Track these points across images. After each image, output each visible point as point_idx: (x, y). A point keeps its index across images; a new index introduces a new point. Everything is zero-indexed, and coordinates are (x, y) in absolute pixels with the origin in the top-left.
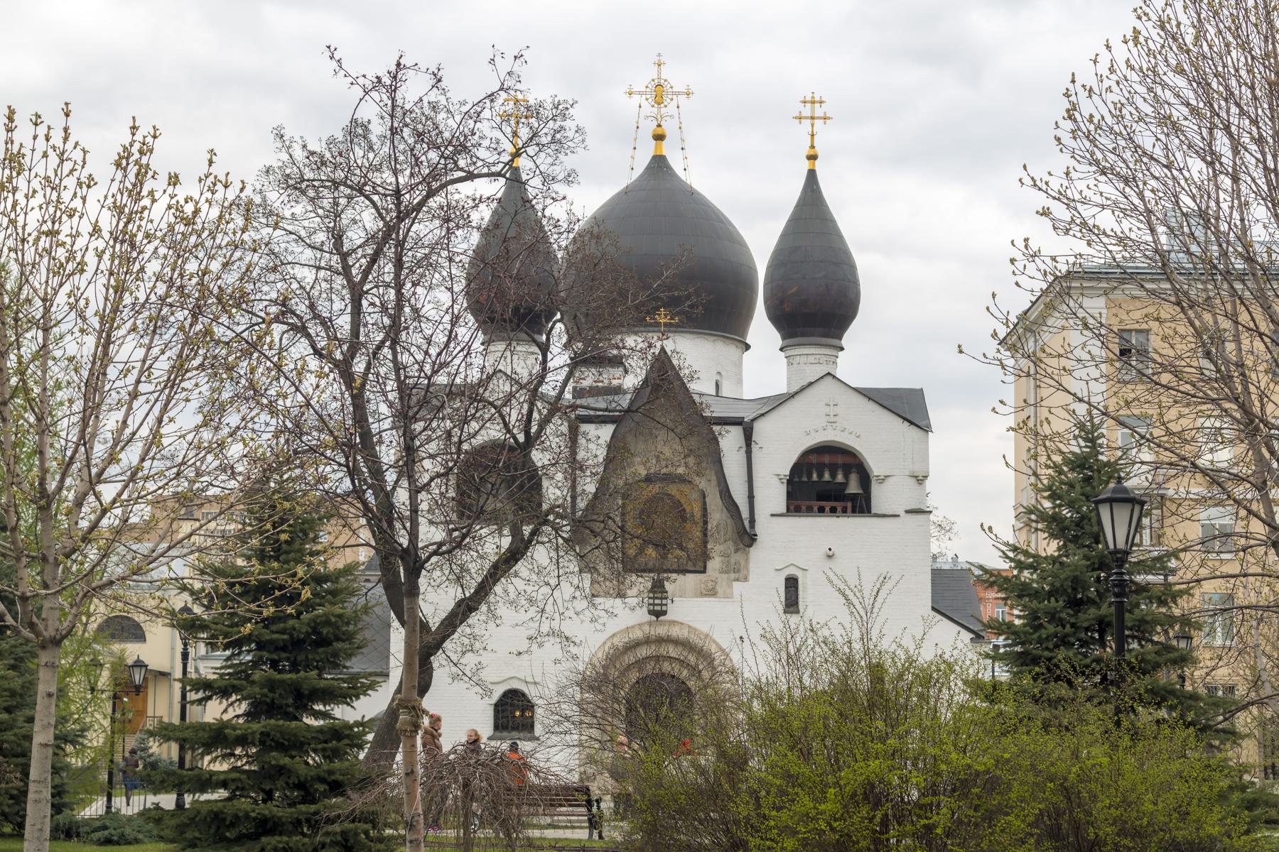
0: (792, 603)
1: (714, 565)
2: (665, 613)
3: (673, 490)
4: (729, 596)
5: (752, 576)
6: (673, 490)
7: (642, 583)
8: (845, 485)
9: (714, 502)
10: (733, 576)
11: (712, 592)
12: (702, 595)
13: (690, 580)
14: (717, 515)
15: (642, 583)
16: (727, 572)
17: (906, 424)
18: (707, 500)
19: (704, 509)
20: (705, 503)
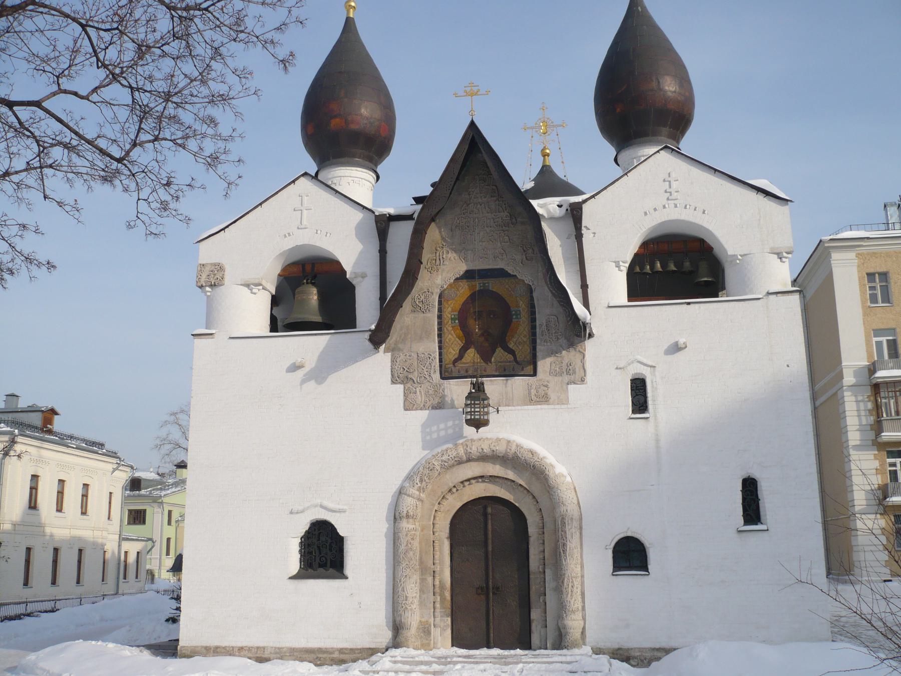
0: (640, 403)
1: (544, 365)
2: (485, 423)
3: (493, 285)
4: (563, 401)
5: (589, 377)
6: (493, 285)
7: (458, 390)
8: (693, 273)
9: (542, 294)
10: (566, 378)
11: (544, 399)
12: (531, 402)
13: (519, 383)
14: (546, 311)
15: (458, 390)
16: (561, 374)
17: (761, 196)
18: (535, 295)
19: (532, 306)
20: (532, 298)
